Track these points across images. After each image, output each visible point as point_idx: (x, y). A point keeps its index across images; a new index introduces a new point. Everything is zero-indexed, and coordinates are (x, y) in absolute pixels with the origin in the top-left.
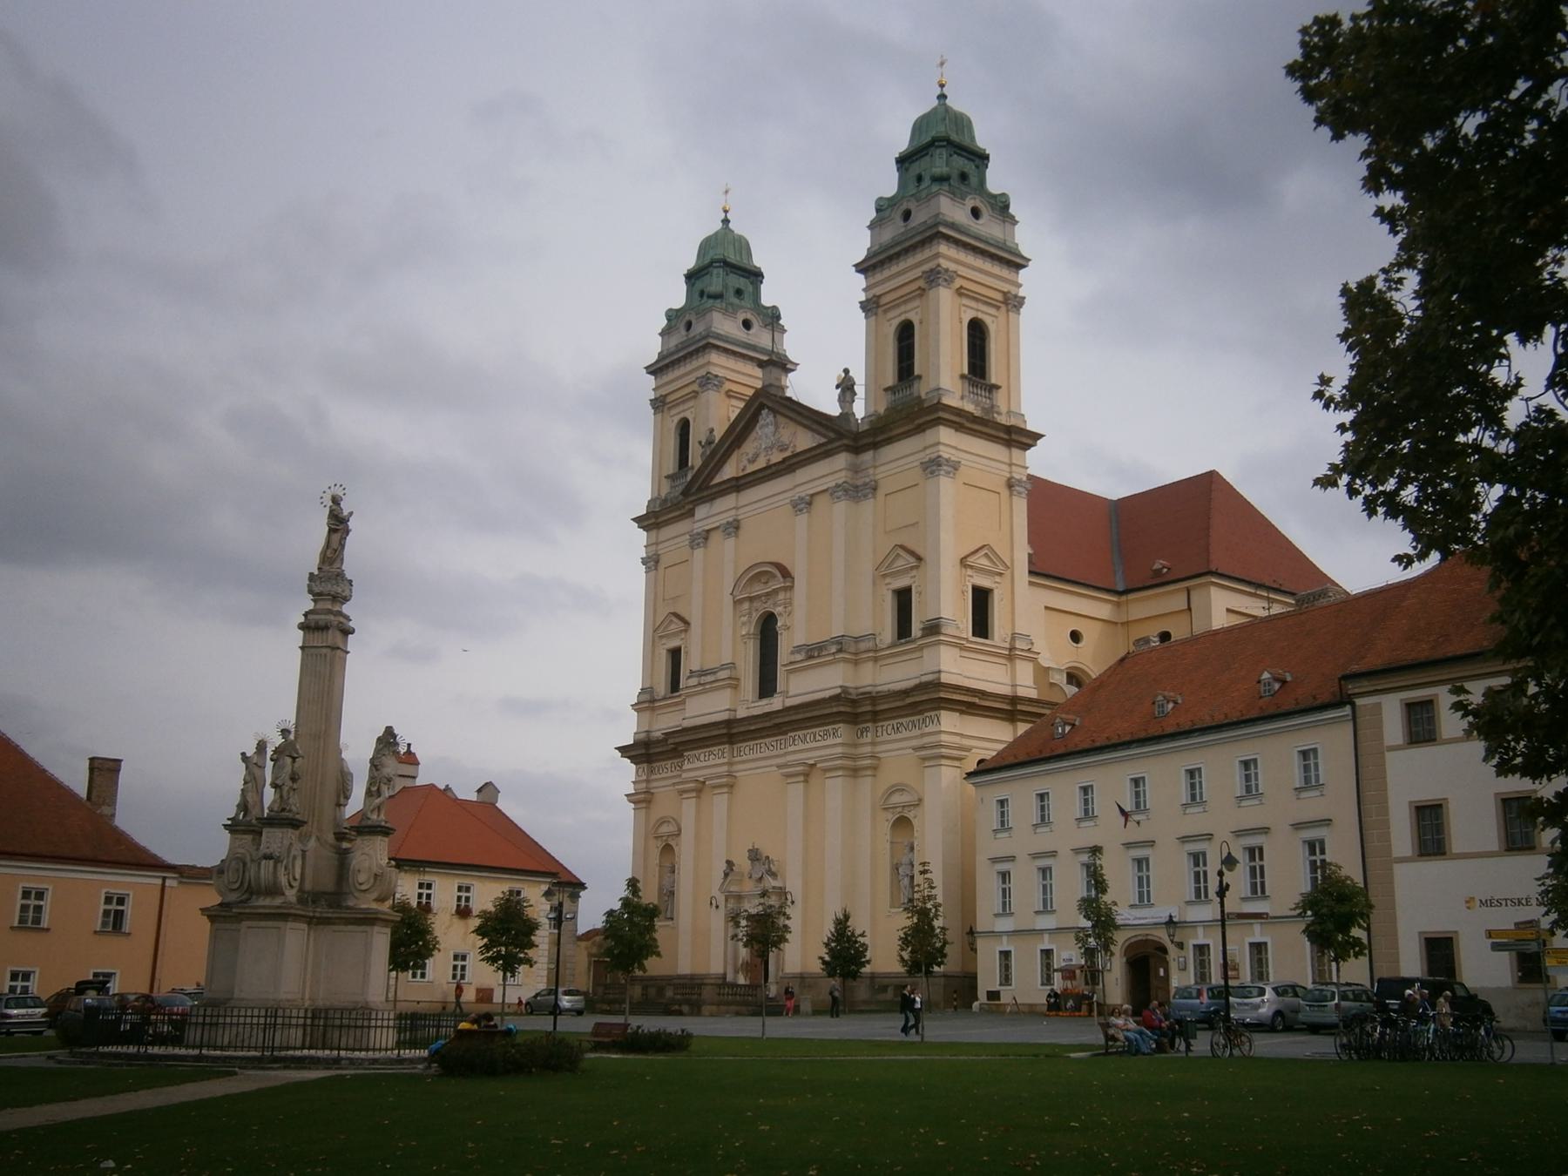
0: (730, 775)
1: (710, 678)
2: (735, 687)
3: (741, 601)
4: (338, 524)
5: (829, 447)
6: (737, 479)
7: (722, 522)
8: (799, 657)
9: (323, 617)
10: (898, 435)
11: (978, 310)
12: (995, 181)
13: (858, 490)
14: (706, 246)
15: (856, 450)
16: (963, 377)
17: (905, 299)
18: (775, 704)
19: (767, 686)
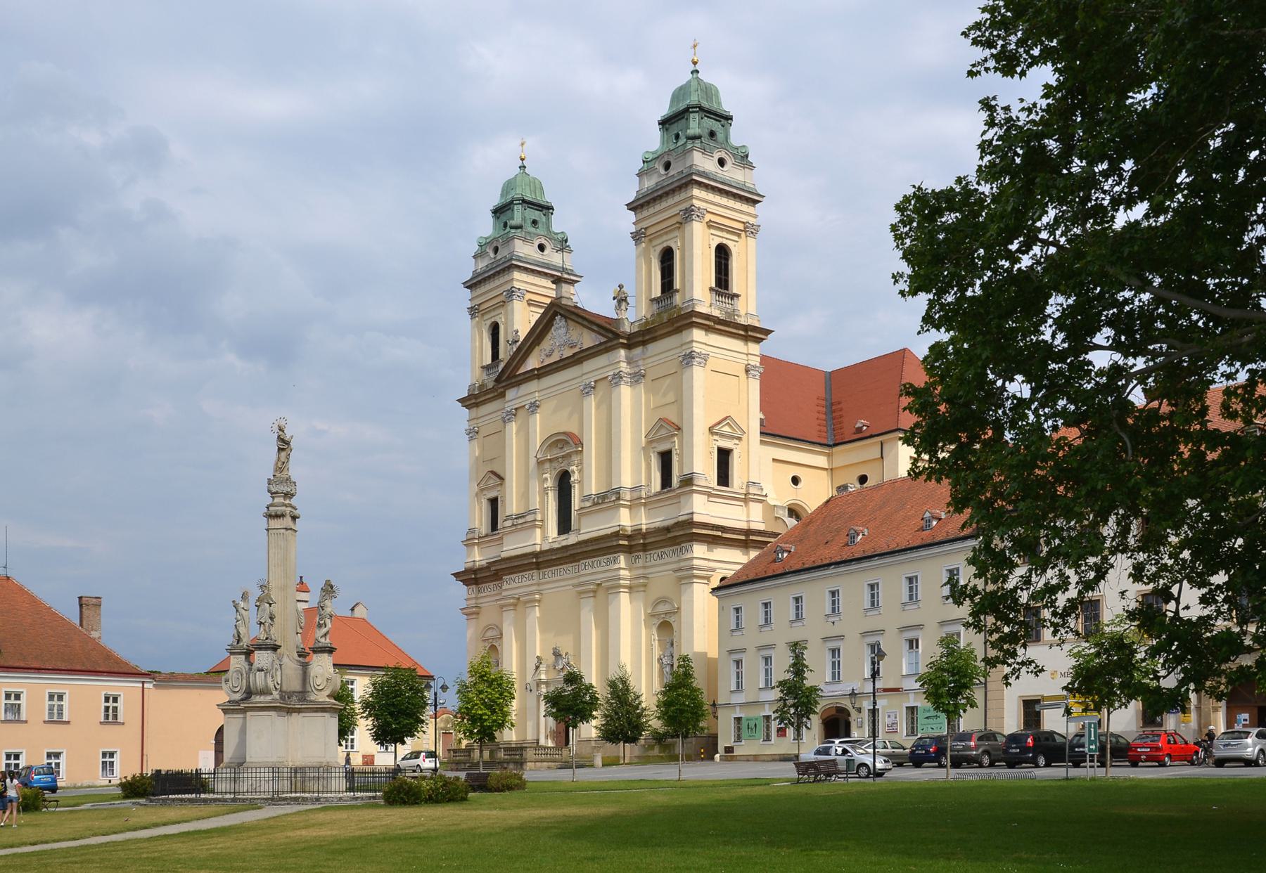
1: (520, 521)
5: (609, 344)
6: (538, 369)
9: (280, 508)
10: (661, 335)
11: (723, 237)
12: (737, 135)
14: (509, 186)
16: (711, 289)
17: (667, 231)
18: (571, 539)
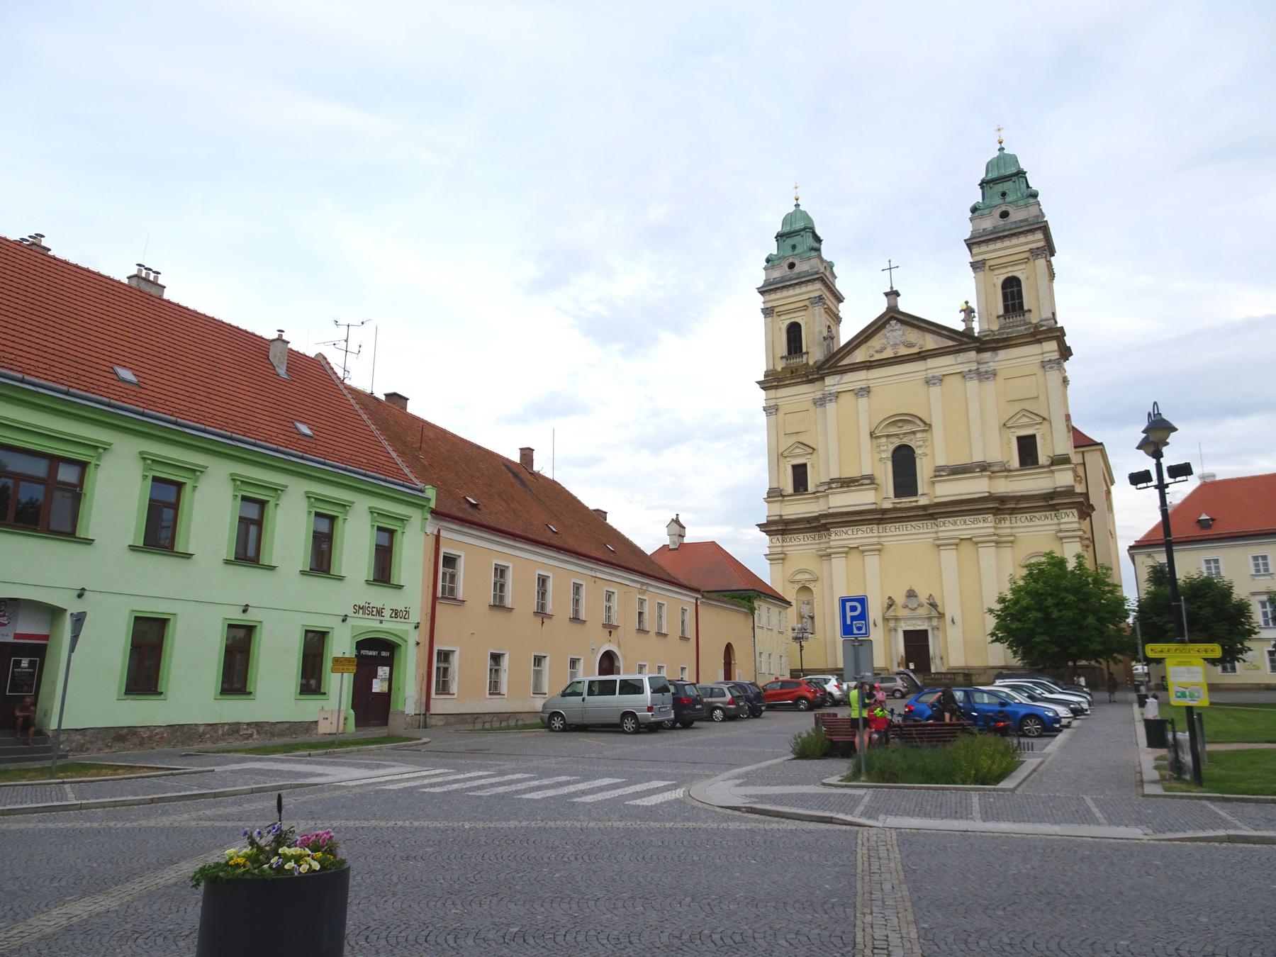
2: (876, 489)
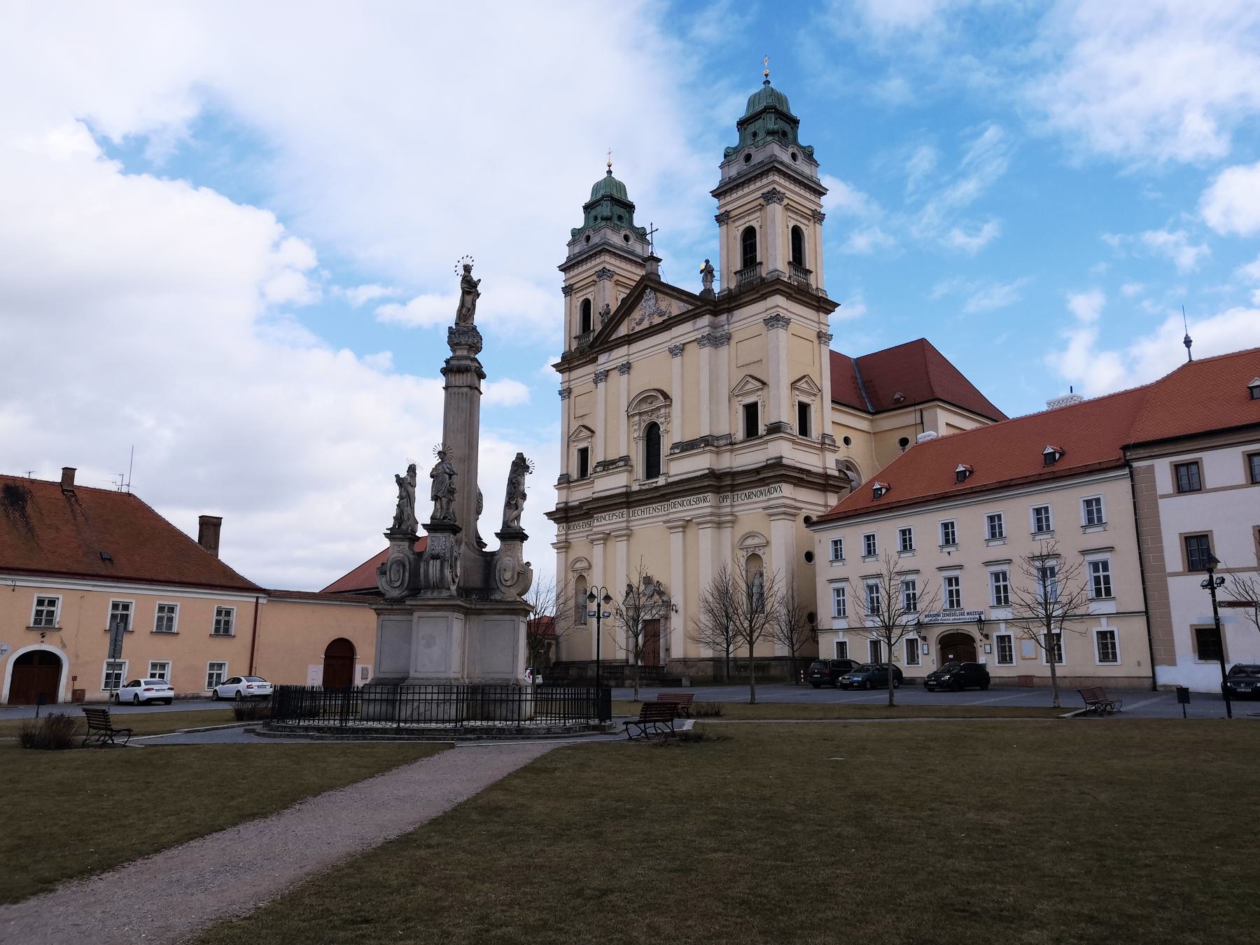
0: (628, 528)
2: (630, 472)
3: (633, 416)
4: (470, 288)
5: (698, 311)
7: (618, 364)
8: (677, 451)
11: (797, 220)
13: (716, 340)
15: (715, 314)
18: (661, 481)
19: (653, 467)
